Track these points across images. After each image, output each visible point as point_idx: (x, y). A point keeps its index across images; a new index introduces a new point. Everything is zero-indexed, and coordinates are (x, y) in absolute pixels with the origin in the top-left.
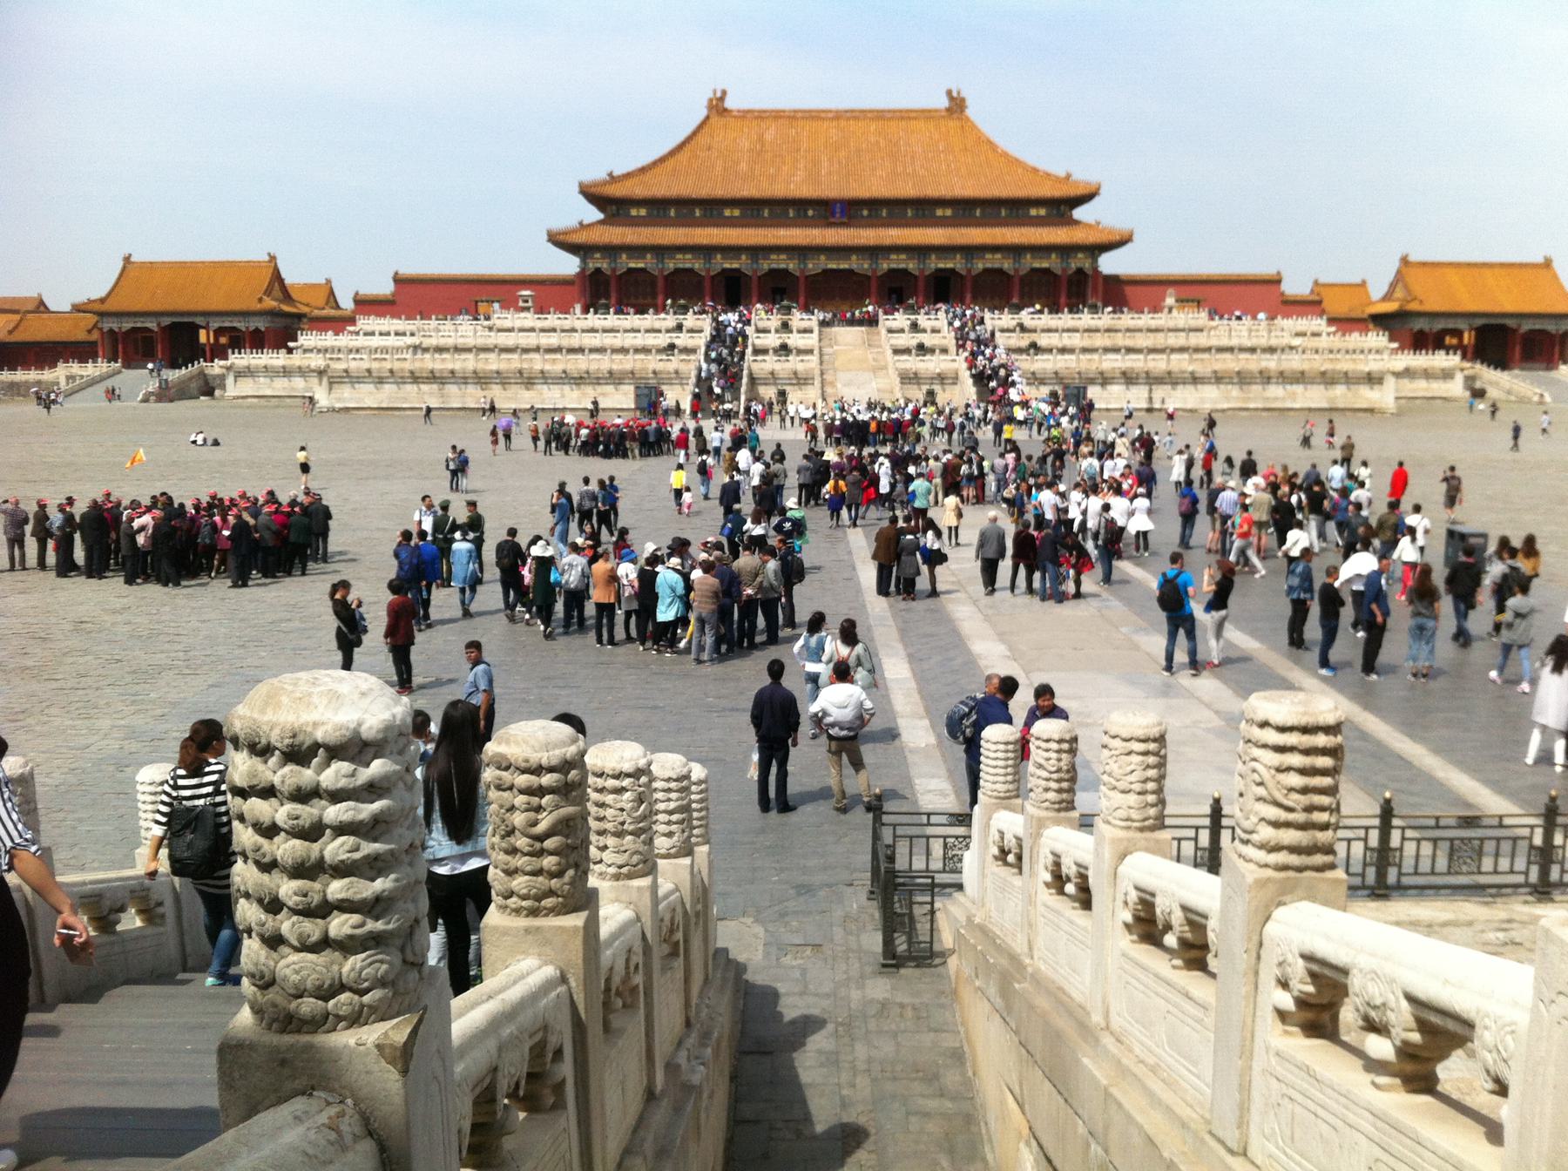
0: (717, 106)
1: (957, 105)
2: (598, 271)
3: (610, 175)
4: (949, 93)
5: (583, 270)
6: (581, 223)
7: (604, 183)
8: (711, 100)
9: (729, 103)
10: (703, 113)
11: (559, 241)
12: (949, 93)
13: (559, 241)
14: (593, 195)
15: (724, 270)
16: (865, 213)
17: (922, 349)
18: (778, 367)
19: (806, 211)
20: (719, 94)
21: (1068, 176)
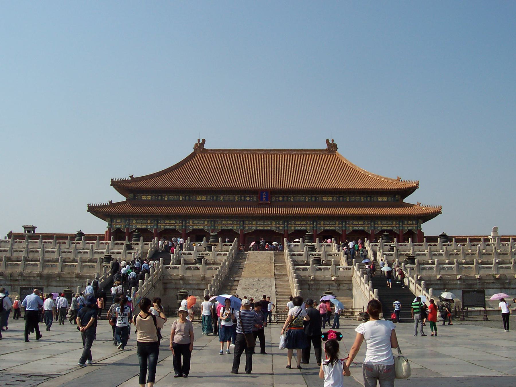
0: (200, 147)
1: (332, 148)
2: (119, 230)
3: (132, 177)
4: (327, 141)
5: (110, 229)
6: (110, 202)
7: (127, 181)
8: (196, 145)
9: (206, 146)
10: (193, 151)
11: (94, 210)
12: (327, 141)
13: (95, 210)
14: (118, 185)
15: (194, 230)
16: (281, 199)
17: (318, 261)
18: (189, 274)
19: (245, 197)
20: (201, 142)
21: (399, 179)
